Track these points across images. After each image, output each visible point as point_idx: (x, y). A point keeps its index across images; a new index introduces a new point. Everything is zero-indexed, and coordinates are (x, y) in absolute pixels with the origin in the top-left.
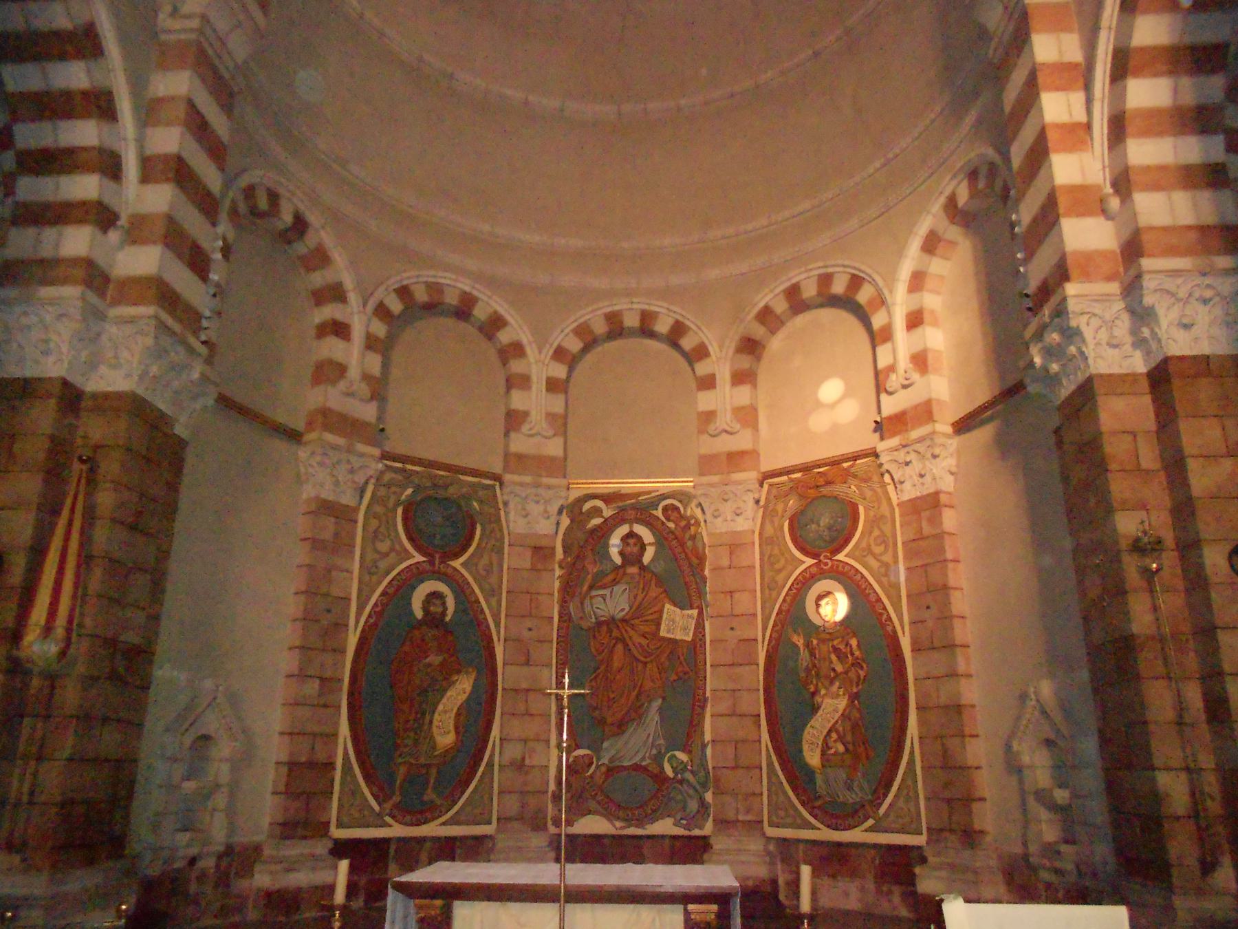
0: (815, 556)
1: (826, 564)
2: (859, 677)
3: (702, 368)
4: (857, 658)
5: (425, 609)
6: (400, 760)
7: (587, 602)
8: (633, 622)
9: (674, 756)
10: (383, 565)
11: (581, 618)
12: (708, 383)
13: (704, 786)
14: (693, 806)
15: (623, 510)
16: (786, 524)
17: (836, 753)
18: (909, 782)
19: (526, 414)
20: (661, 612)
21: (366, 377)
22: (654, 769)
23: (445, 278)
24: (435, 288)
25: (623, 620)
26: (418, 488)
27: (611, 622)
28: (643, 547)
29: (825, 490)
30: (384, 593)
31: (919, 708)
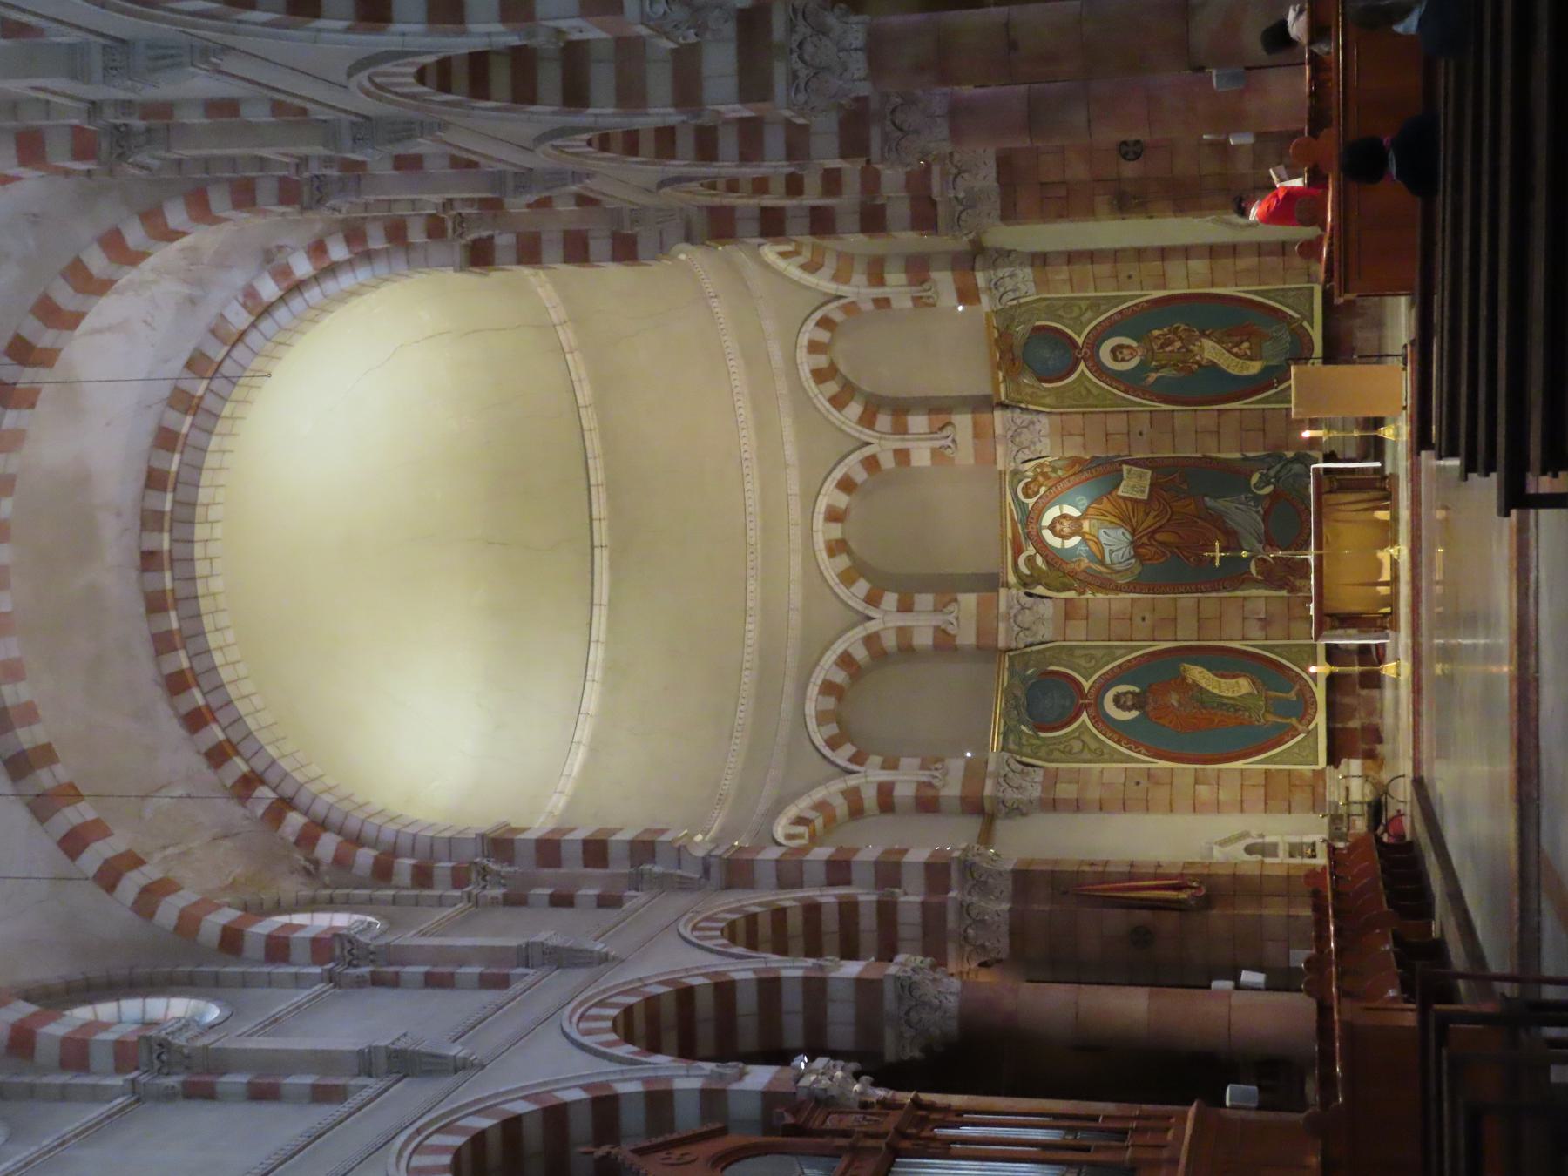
1: (1086, 353)
2: (1185, 330)
3: (887, 461)
4: (1169, 331)
5: (1129, 709)
6: (1262, 721)
7: (1117, 567)
8: (1135, 524)
9: (1255, 485)
10: (1093, 745)
11: (1132, 573)
12: (902, 456)
13: (1280, 458)
14: (1297, 468)
15: (1028, 536)
16: (1046, 385)
17: (1250, 348)
18: (1272, 295)
19: (937, 629)
20: (1125, 499)
21: (923, 767)
22: (1267, 504)
23: (810, 709)
24: (822, 718)
25: (1134, 532)
26: (1021, 722)
28: (1064, 516)
29: (1018, 352)
30: (1118, 742)
31: (1213, 285)
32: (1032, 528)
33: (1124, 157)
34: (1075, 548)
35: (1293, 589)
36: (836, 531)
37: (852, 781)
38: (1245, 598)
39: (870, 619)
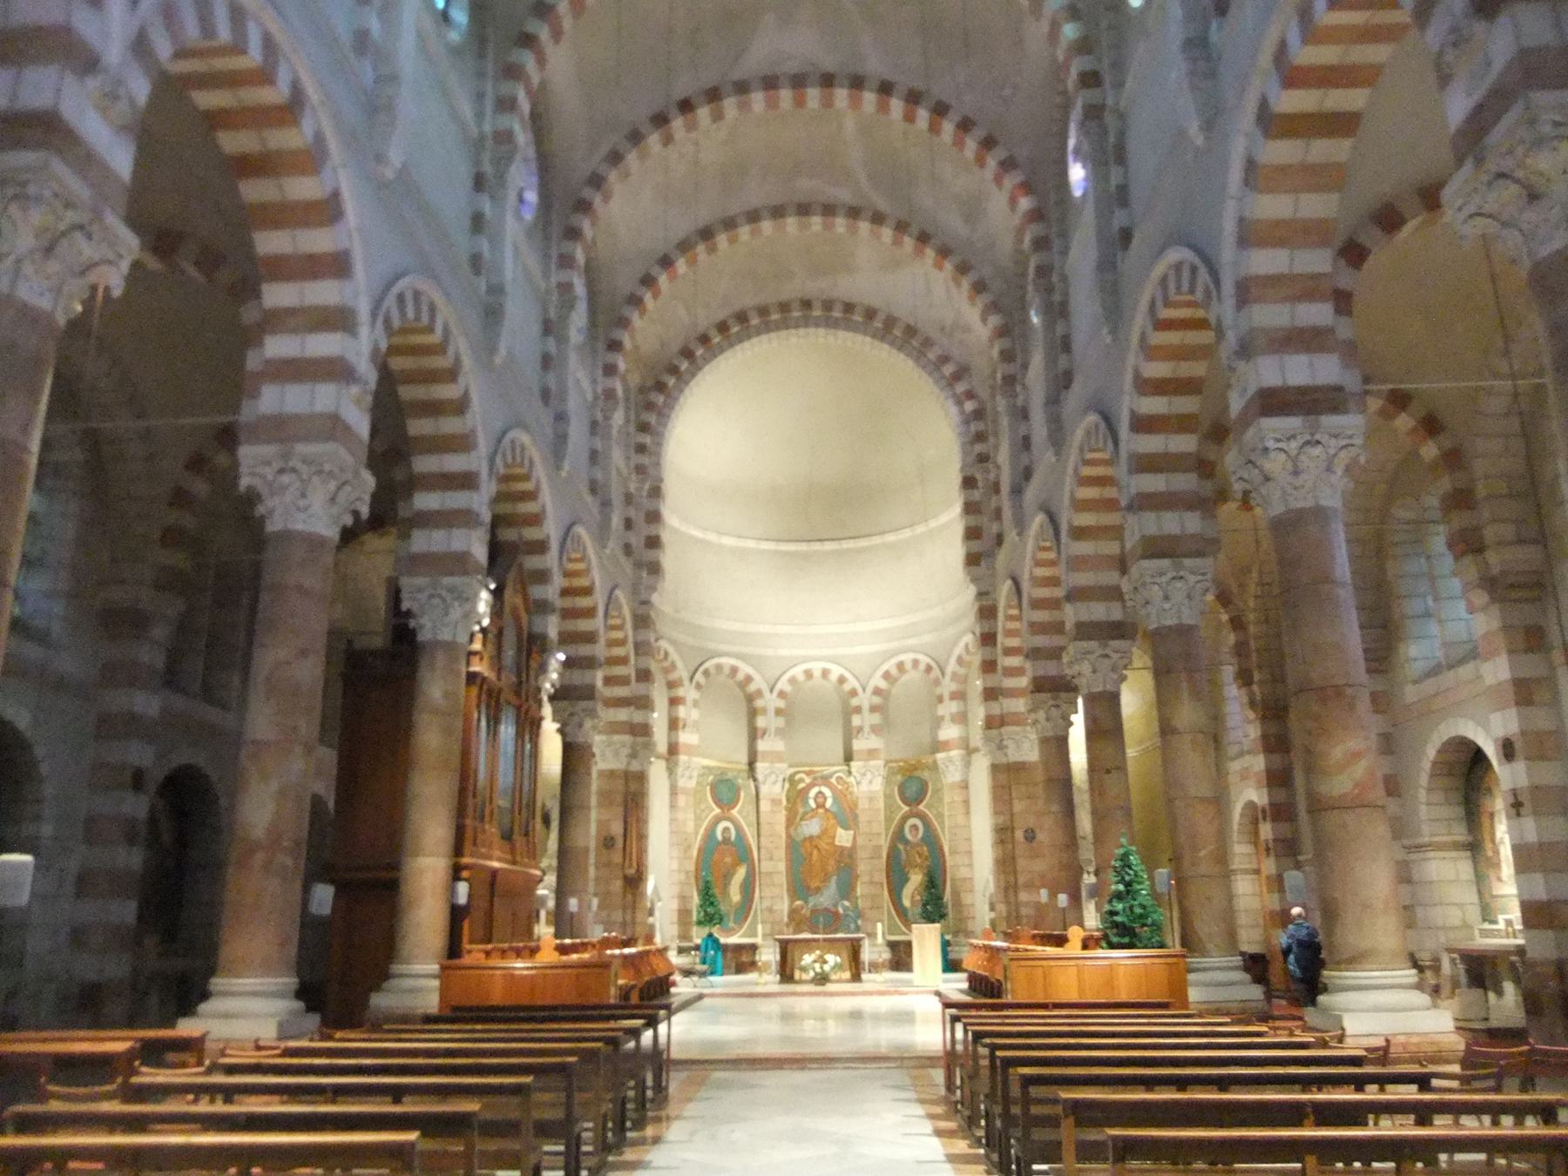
0: (909, 805)
10: (703, 816)
14: (852, 926)
22: (833, 909)
27: (811, 838)
28: (825, 799)
32: (819, 781)
33: (1026, 831)
34: (807, 803)
35: (788, 925)
36: (817, 674)
37: (686, 682)
38: (782, 898)
39: (771, 691)
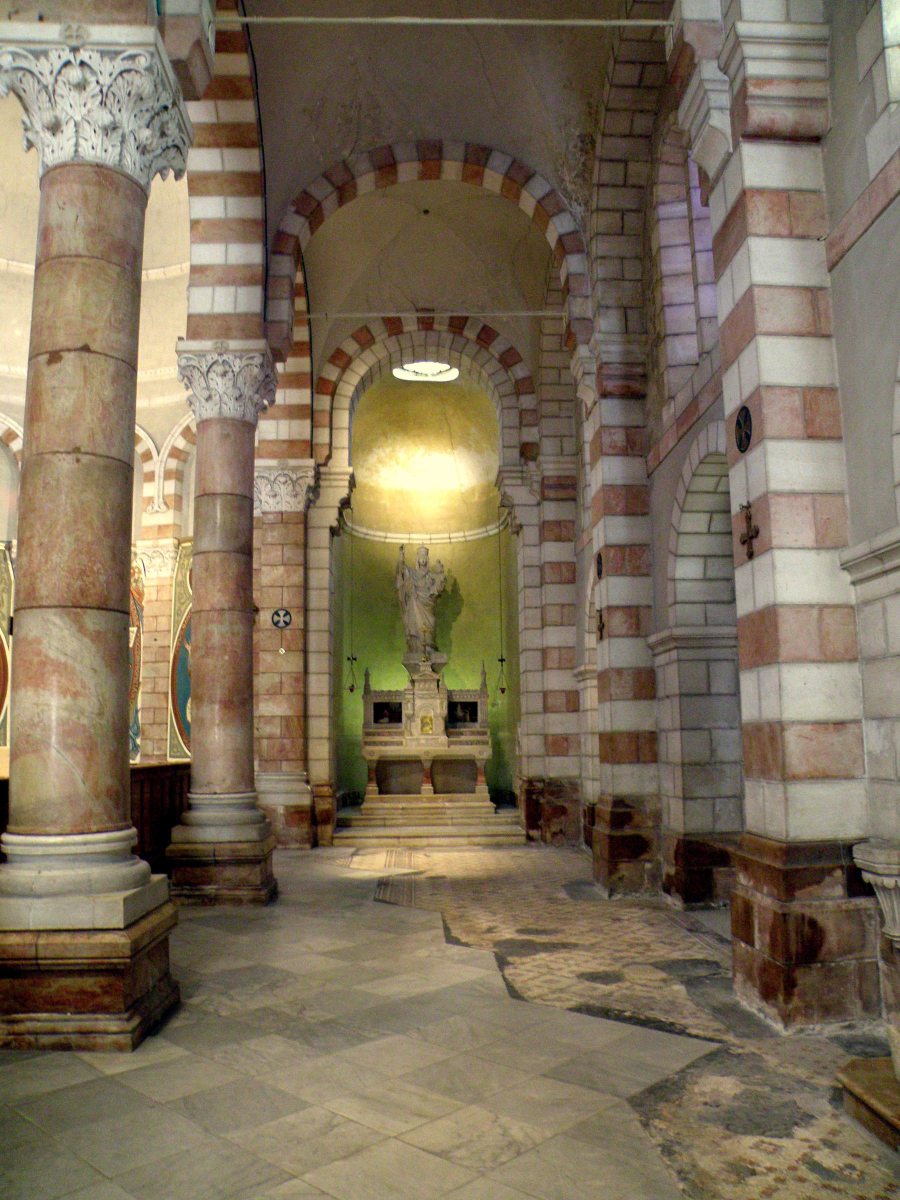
33: (277, 613)
